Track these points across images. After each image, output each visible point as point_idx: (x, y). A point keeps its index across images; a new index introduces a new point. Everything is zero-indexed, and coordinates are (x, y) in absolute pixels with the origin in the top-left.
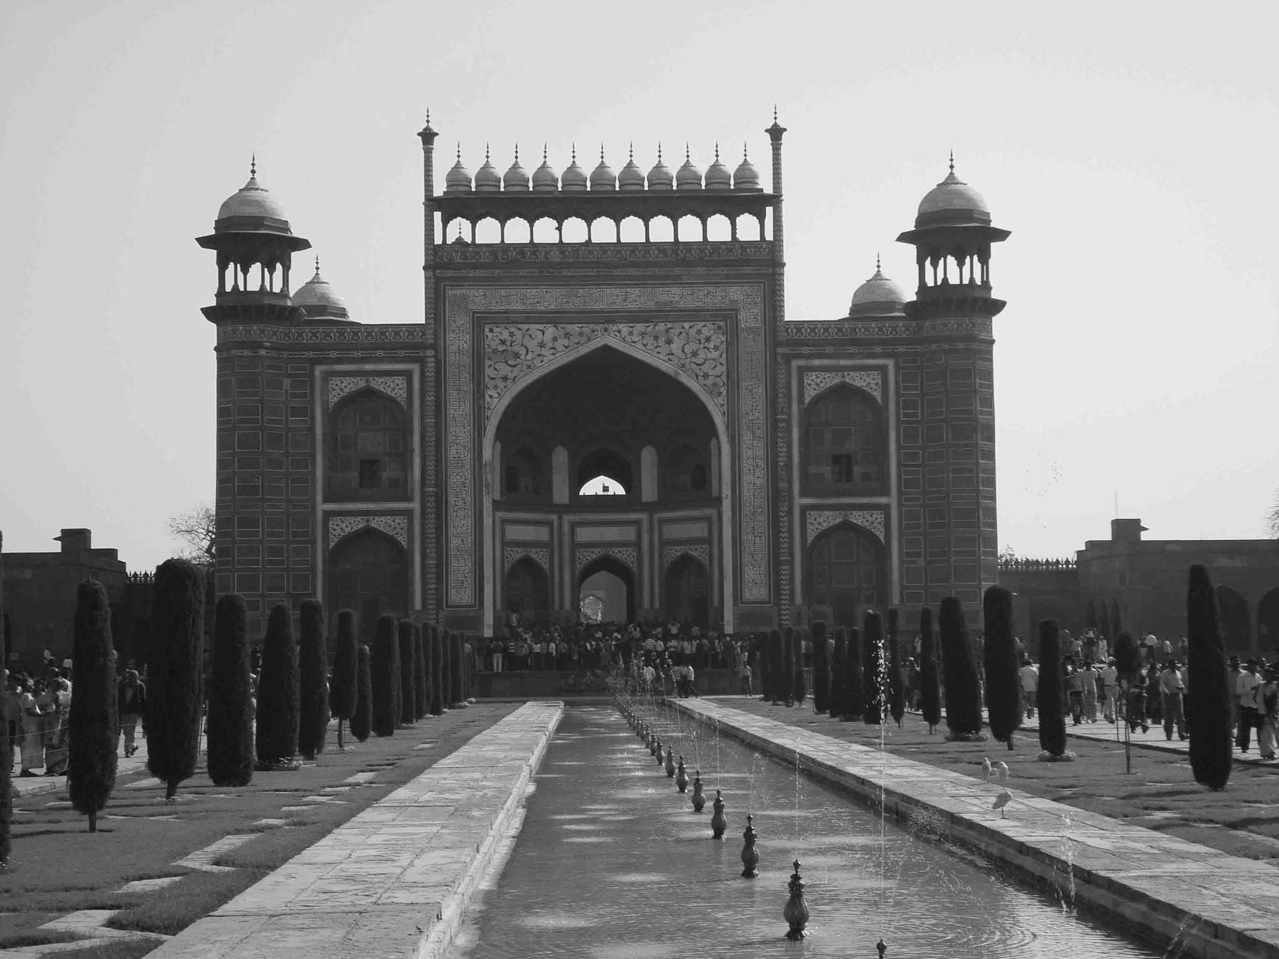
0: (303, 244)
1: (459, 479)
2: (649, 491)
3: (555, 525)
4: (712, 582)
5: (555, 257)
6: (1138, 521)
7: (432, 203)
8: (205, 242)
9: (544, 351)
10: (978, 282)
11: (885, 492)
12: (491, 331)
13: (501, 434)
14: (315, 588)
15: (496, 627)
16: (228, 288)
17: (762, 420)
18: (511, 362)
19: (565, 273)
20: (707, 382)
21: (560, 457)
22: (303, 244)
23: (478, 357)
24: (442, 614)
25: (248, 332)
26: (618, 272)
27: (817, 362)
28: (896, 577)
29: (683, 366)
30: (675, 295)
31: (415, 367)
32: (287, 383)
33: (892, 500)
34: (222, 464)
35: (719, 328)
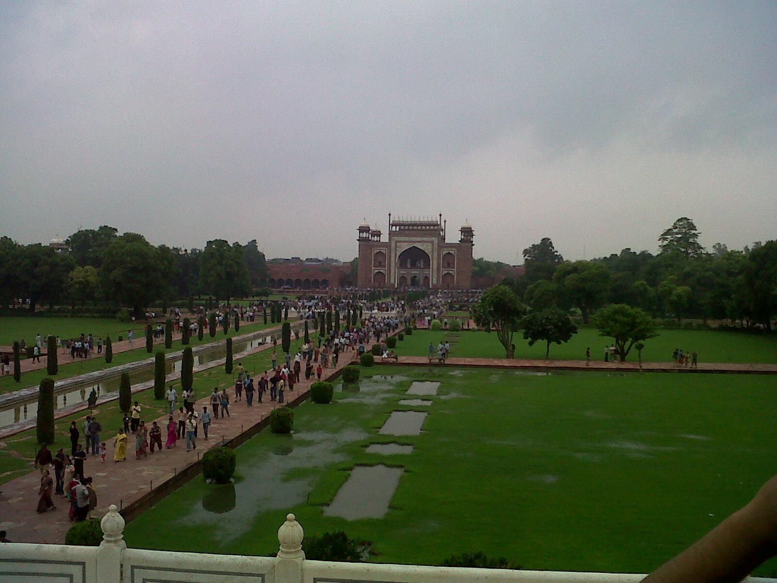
1: (393, 264)
2: (422, 266)
11: (454, 268)
23: (396, 246)
30: (425, 239)
33: (455, 269)
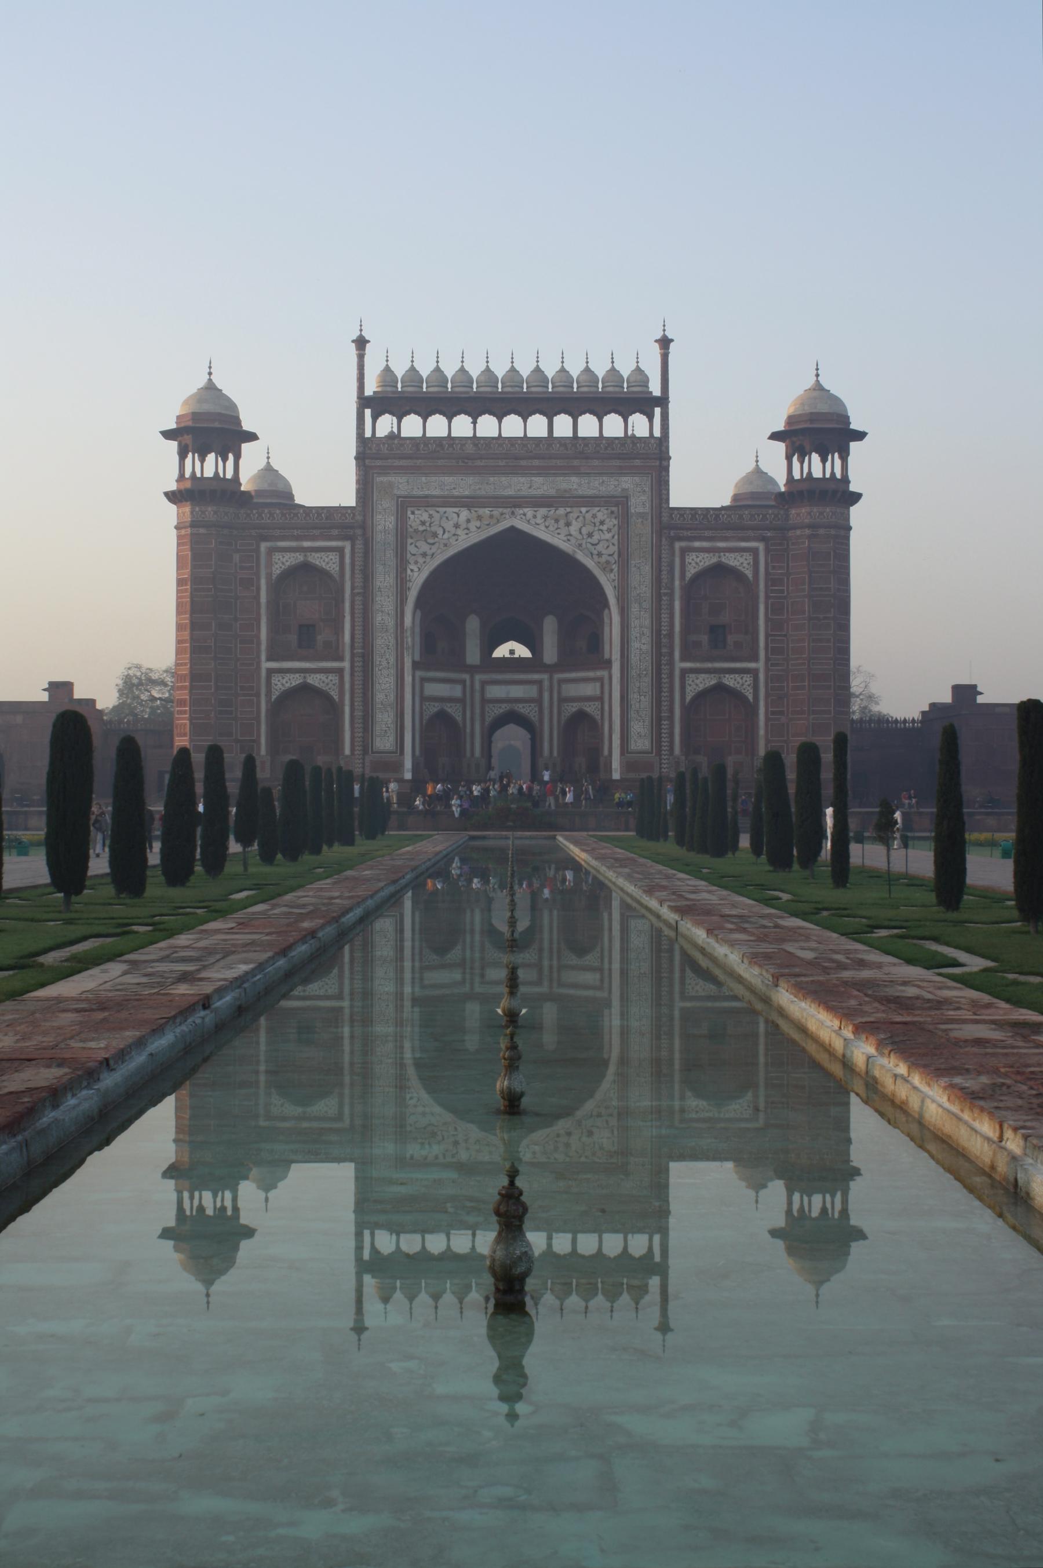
0: (252, 437)
1: (384, 643)
2: (550, 655)
3: (468, 683)
4: (603, 734)
5: (470, 449)
6: (975, 687)
7: (364, 402)
8: (168, 435)
9: (459, 532)
10: (838, 476)
11: (756, 659)
12: (413, 513)
13: (419, 604)
14: (259, 736)
15: (415, 769)
16: (188, 474)
17: (649, 595)
18: (431, 541)
19: (478, 463)
20: (600, 560)
21: (473, 624)
22: (252, 437)
23: (402, 534)
24: (368, 759)
25: (203, 512)
26: (523, 463)
27: (697, 544)
28: (762, 732)
29: (580, 545)
30: (573, 484)
31: (347, 545)
32: (236, 557)
33: (761, 665)
34: (180, 627)
35: (612, 512)
